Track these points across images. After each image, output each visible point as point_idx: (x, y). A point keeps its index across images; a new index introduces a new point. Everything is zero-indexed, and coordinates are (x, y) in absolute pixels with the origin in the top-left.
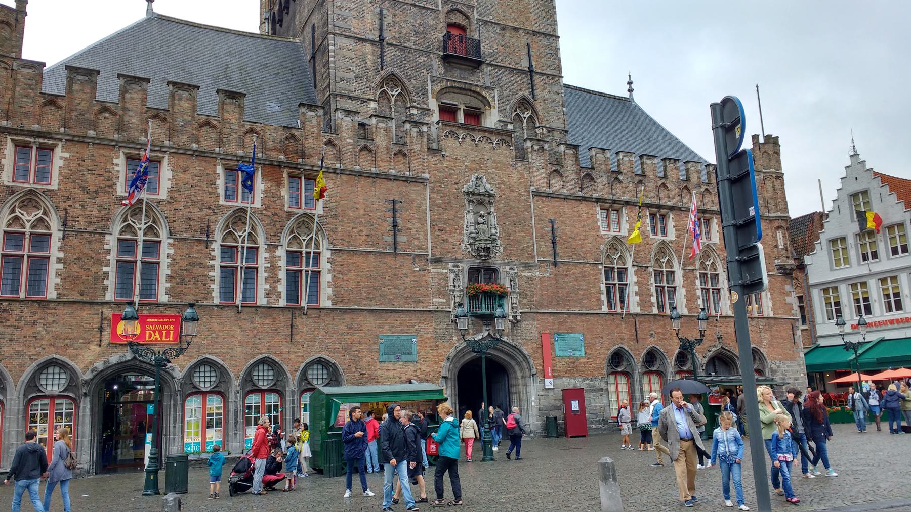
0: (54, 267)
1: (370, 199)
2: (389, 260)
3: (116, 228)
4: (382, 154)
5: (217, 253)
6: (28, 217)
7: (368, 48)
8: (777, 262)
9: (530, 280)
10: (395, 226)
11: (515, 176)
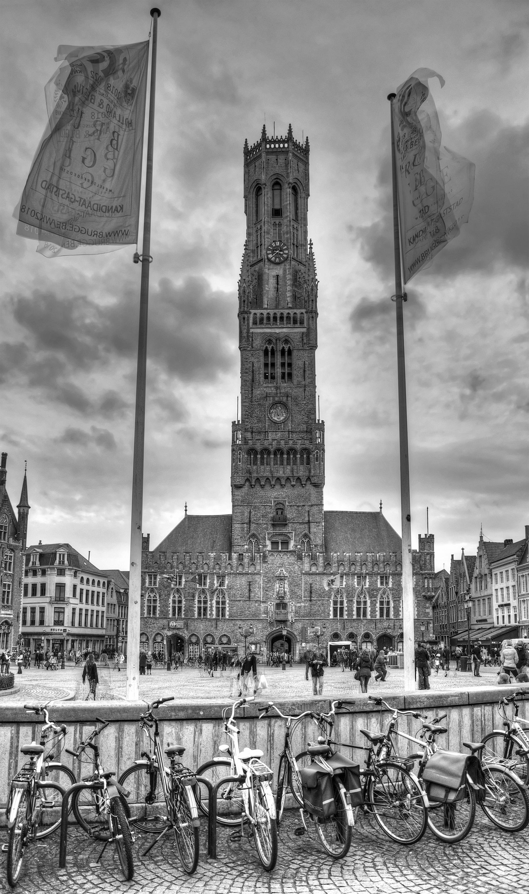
0: (158, 608)
1: (242, 581)
2: (248, 603)
3: (172, 597)
4: (246, 565)
5: (196, 603)
6: (152, 595)
7: (245, 525)
8: (423, 593)
9: (300, 607)
10: (250, 590)
11: (296, 567)
